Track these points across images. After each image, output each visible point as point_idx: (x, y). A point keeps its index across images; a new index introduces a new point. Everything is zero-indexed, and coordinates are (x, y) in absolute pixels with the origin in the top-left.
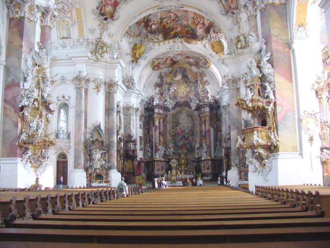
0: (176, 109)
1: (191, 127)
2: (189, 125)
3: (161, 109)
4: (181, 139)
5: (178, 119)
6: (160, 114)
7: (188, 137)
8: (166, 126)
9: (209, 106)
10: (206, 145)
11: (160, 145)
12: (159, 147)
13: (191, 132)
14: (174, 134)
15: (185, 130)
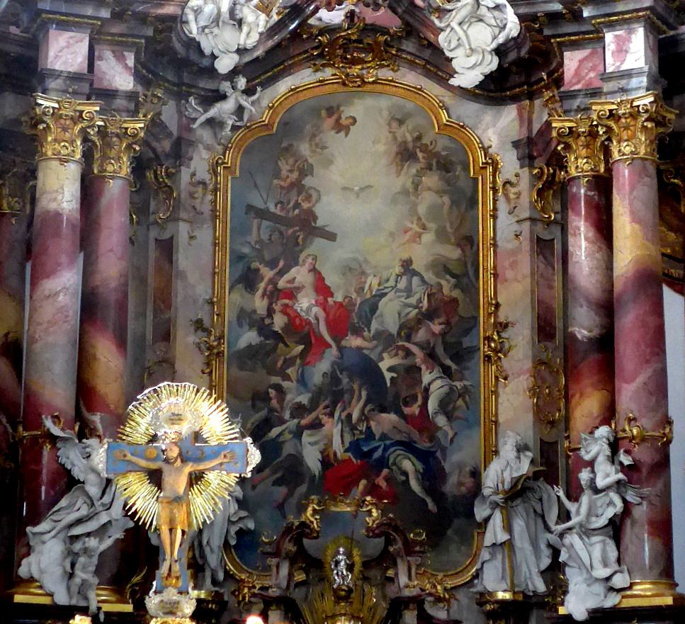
0: (283, 86)
1: (442, 267)
2: (424, 252)
3: (119, 46)
4: (332, 394)
5: (298, 186)
6: (107, 95)
7: (412, 372)
8: (167, 248)
9: (652, 28)
10: (614, 446)
11: (85, 431)
12: (71, 457)
13: (437, 328)
14: (250, 337)
15: (372, 306)
